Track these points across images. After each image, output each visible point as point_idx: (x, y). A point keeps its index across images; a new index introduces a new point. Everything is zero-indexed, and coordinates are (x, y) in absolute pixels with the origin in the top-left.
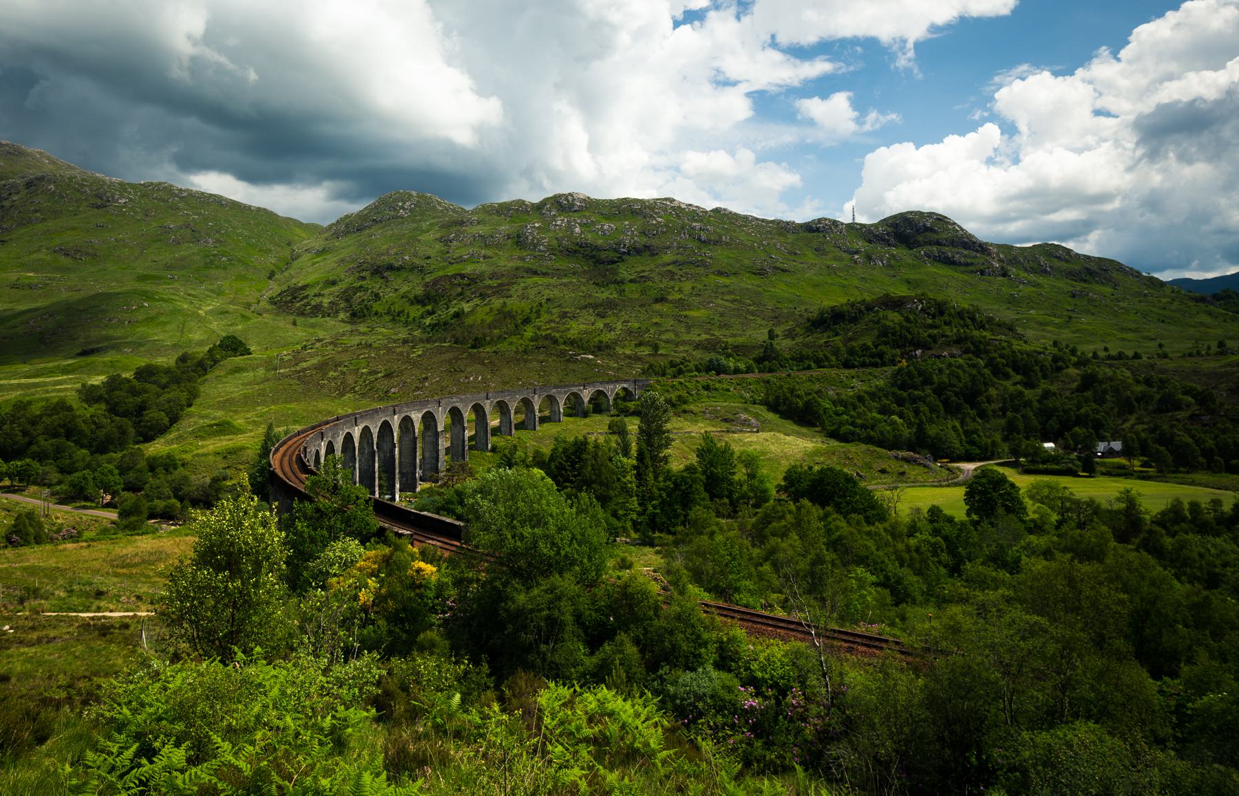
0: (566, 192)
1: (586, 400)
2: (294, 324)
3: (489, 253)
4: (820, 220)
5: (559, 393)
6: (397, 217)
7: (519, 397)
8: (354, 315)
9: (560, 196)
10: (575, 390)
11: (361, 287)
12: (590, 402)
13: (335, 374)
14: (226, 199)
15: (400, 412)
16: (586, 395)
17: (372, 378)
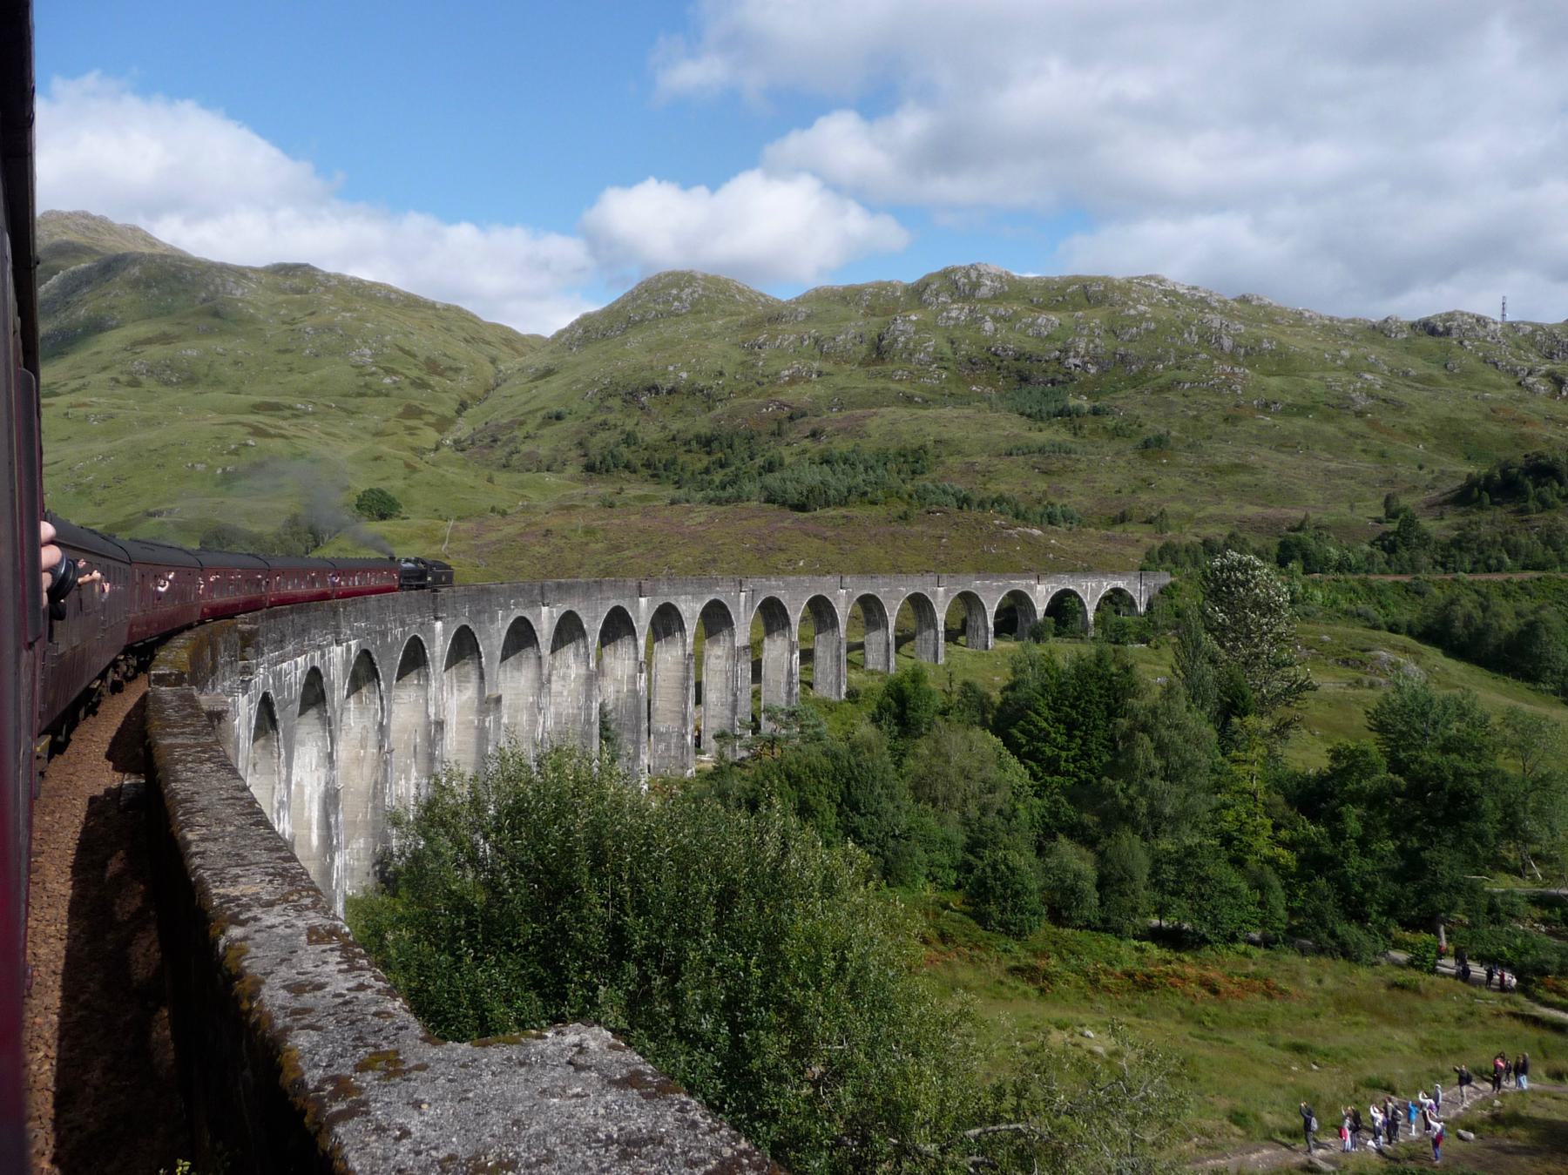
0: (966, 263)
1: (1041, 608)
2: (490, 480)
3: (828, 367)
4: (1451, 316)
5: (988, 589)
6: (670, 314)
7: (906, 591)
8: (590, 468)
9: (954, 270)
10: (1019, 584)
11: (605, 423)
12: (1048, 612)
13: (545, 550)
14: (397, 292)
15: (653, 593)
16: (1041, 595)
17: (613, 558)
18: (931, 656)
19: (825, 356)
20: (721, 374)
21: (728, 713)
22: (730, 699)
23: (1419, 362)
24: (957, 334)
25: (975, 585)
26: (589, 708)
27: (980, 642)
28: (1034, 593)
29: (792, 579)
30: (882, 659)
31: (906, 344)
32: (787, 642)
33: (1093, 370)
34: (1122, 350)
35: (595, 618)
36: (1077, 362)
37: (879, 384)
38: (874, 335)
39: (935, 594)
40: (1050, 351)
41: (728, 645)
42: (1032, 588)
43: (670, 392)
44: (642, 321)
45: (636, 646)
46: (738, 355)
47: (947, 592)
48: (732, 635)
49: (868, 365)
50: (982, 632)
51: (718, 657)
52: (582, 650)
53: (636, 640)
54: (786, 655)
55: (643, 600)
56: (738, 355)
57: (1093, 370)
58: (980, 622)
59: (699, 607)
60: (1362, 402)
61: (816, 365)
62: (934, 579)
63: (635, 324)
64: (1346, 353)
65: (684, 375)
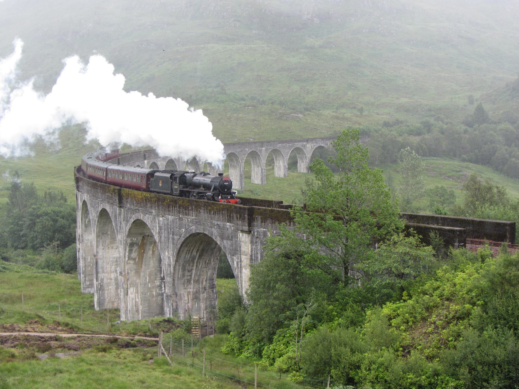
39: (261, 151)
42: (304, 146)
47: (266, 150)
55: (146, 161)
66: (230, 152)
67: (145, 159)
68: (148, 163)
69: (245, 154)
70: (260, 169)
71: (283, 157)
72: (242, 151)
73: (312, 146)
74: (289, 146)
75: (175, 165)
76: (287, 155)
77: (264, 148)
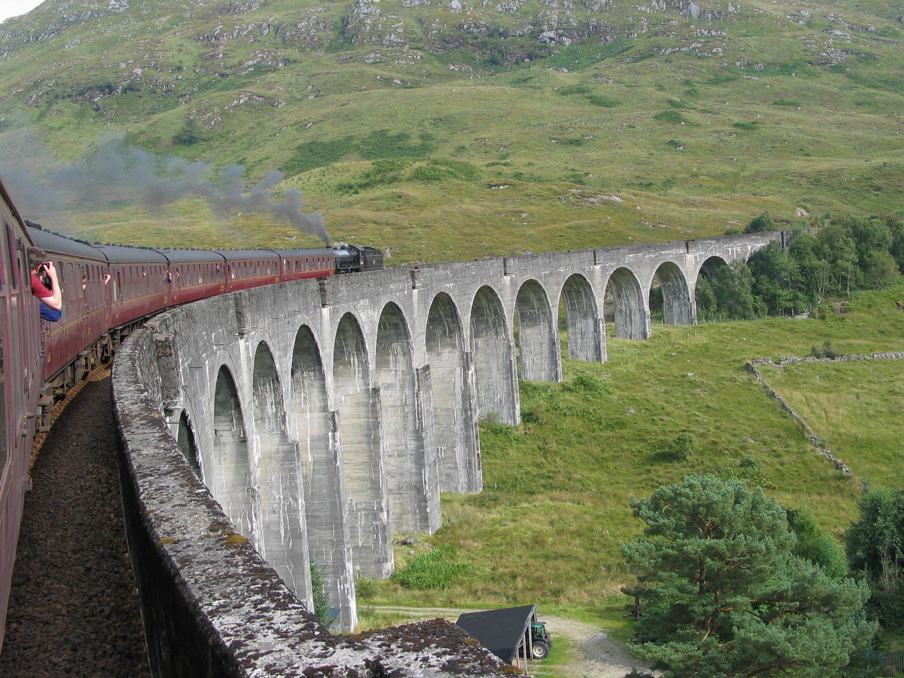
7: (566, 272)
10: (669, 255)
18: (591, 353)
19: (287, 43)
20: (179, 69)
21: (410, 465)
22: (412, 445)
23: (873, 18)
24: (425, 13)
25: (628, 260)
26: (292, 511)
27: (636, 329)
28: (684, 265)
29: (458, 266)
30: (546, 364)
31: (374, 25)
32: (457, 354)
33: (567, 42)
34: (593, 21)
35: (285, 350)
36: (552, 34)
37: (353, 67)
38: (337, 19)
39: (592, 272)
40: (522, 26)
41: (402, 367)
42: (681, 258)
43: (129, 89)
44: (77, 22)
45: (323, 389)
46: (195, 48)
47: (604, 269)
48: (407, 353)
49: (337, 49)
50: (637, 318)
51: (389, 386)
52: (270, 410)
53: (323, 378)
54: (459, 371)
55: (326, 311)
56: (195, 48)
57: (567, 42)
58: (633, 304)
59: (376, 316)
60: (838, 57)
61: (281, 53)
62: (590, 255)
63: (70, 24)
64: (806, 13)
65: (139, 71)
66: (527, 277)
67: (324, 305)
68: (332, 319)
69: (558, 284)
70: (591, 321)
71: (638, 287)
72: (551, 274)
73: (695, 258)
74: (650, 259)
75: (403, 320)
76: (647, 282)
77: (598, 267)
